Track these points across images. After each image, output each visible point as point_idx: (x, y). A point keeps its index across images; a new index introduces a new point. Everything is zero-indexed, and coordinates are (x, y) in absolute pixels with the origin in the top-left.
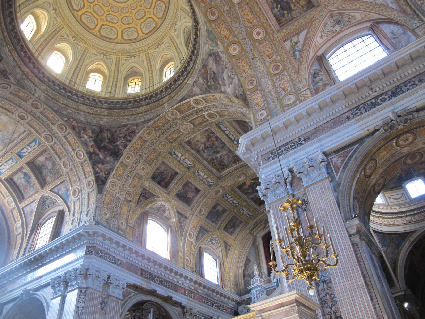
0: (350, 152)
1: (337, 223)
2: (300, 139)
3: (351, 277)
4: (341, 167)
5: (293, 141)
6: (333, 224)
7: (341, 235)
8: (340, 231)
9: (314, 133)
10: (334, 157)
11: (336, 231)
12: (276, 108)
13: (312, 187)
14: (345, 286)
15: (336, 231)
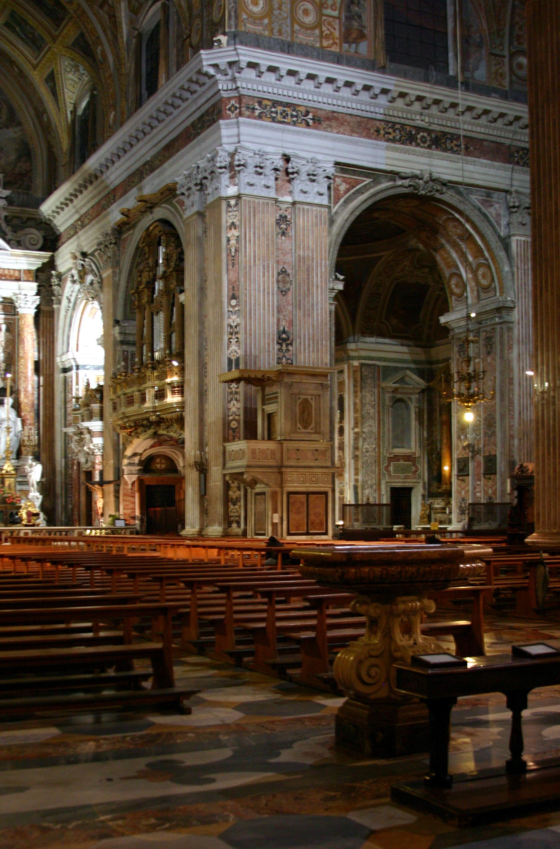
0: (359, 184)
1: (321, 277)
2: (307, 113)
3: (318, 349)
4: (342, 197)
5: (298, 109)
6: (317, 276)
7: (322, 293)
8: (322, 290)
9: (328, 119)
10: (339, 177)
11: (317, 287)
12: (280, 8)
13: (306, 207)
14: (309, 357)
15: (317, 287)
